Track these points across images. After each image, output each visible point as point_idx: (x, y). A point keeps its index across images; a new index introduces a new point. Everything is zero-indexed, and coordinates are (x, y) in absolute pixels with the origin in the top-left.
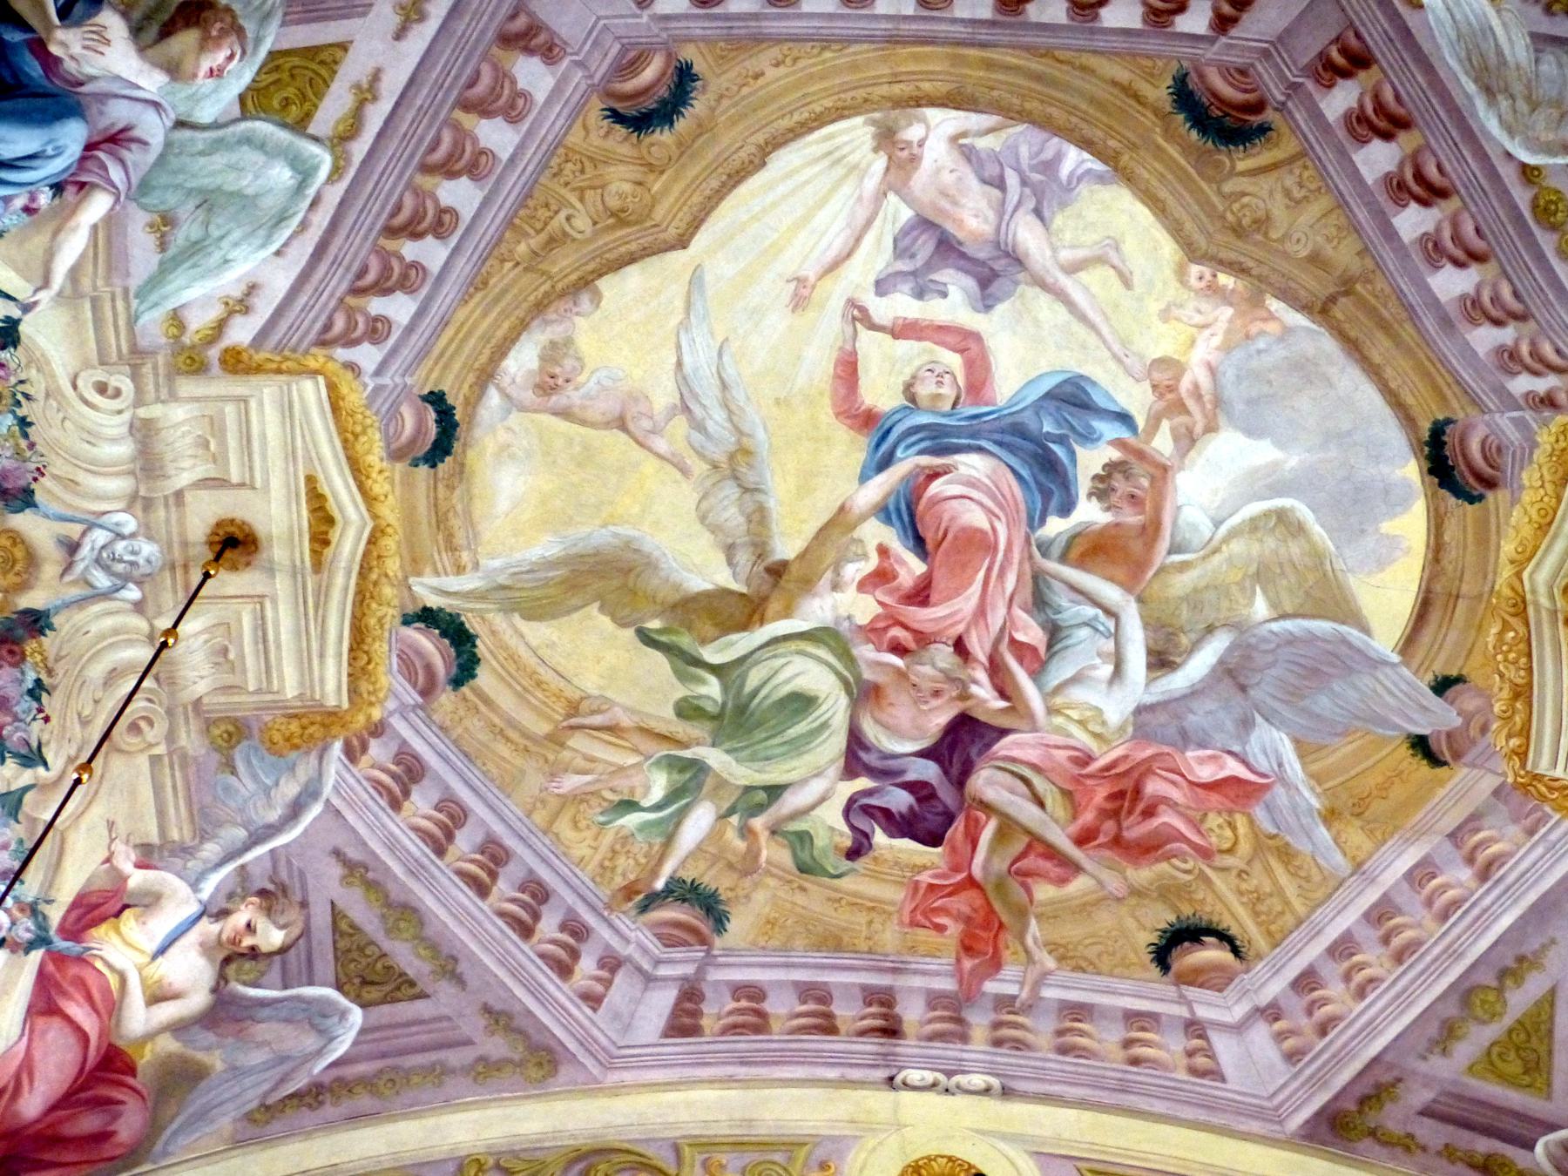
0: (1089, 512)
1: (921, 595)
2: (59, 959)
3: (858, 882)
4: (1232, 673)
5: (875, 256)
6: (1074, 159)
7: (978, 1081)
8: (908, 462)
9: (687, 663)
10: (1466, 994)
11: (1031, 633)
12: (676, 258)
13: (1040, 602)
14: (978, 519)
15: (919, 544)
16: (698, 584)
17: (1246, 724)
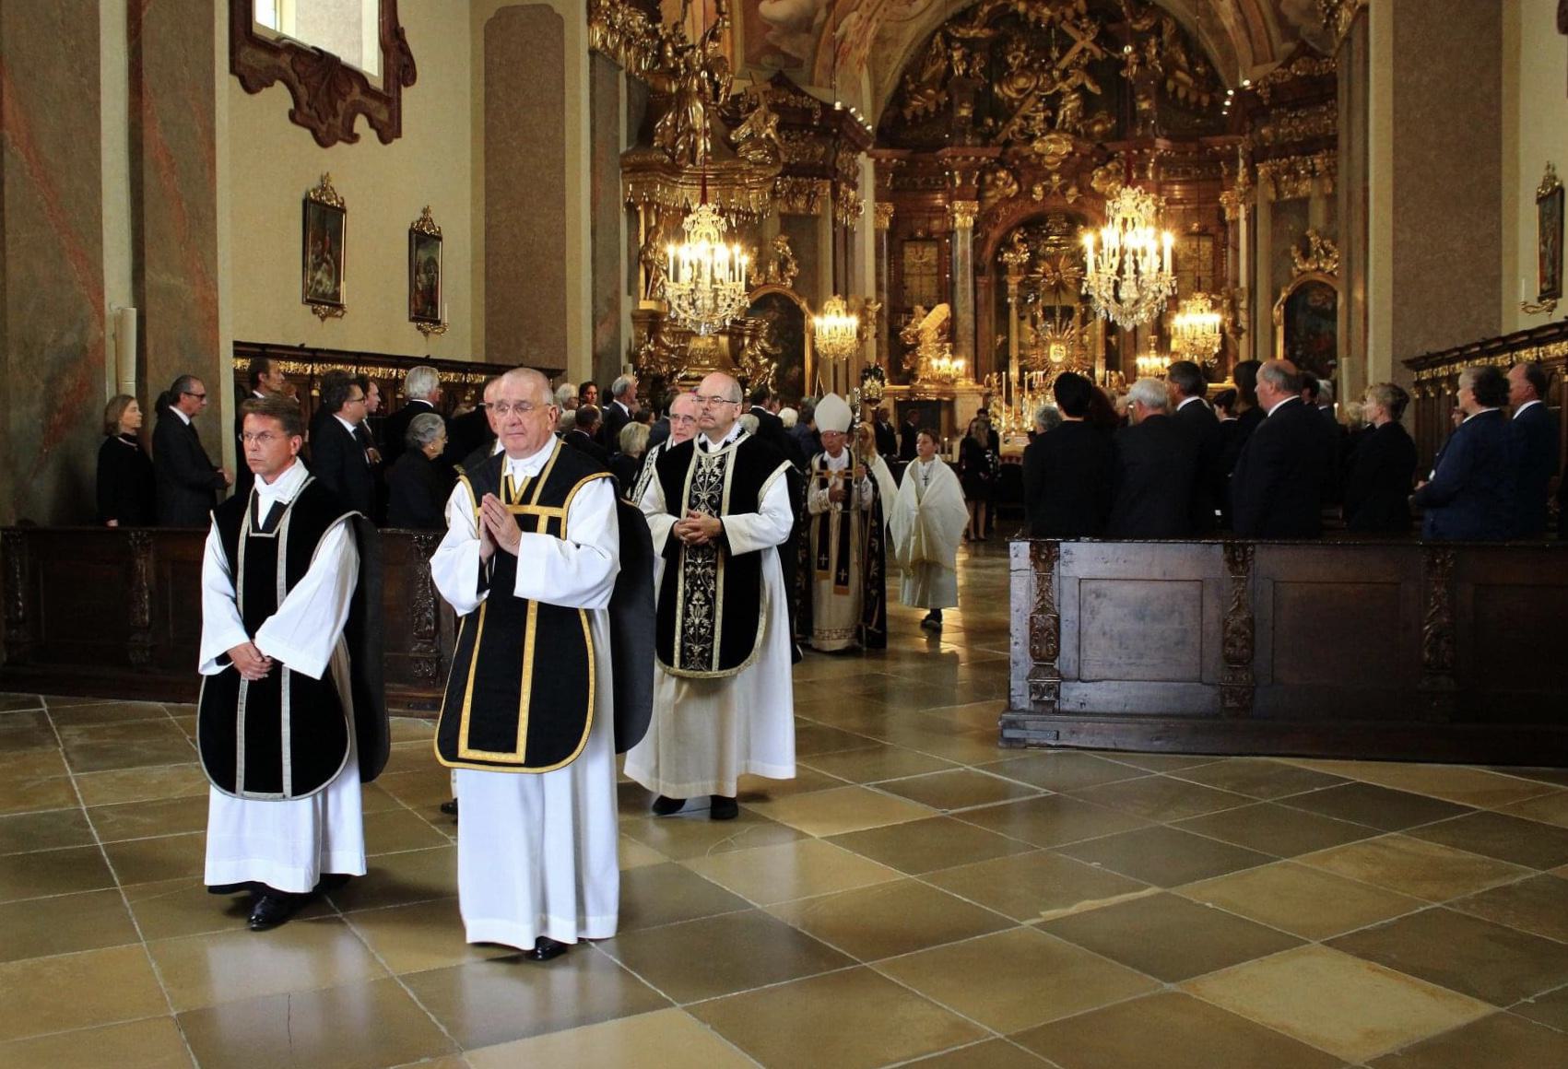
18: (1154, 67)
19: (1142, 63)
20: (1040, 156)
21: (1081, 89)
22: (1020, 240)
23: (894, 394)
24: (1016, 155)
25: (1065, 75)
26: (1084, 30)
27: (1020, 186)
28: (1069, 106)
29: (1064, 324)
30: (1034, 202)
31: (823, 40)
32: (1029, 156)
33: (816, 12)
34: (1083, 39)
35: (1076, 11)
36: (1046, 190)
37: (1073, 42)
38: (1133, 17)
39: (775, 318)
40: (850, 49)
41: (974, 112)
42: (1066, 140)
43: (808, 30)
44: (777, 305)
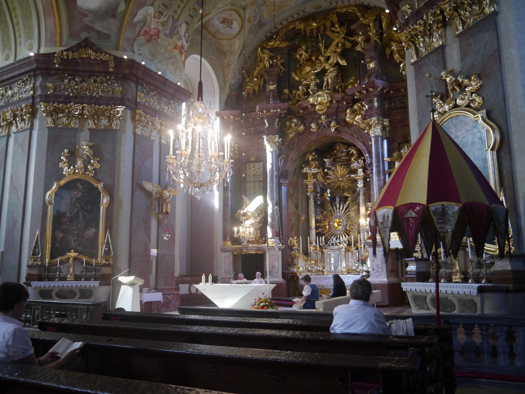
18: (374, 40)
19: (367, 40)
20: (313, 105)
21: (337, 64)
22: (313, 159)
23: (233, 251)
24: (300, 106)
25: (328, 59)
26: (338, 33)
27: (305, 125)
28: (331, 75)
29: (341, 207)
30: (313, 133)
31: (125, 22)
32: (307, 106)
34: (338, 37)
35: (332, 22)
36: (319, 126)
37: (332, 41)
38: (363, 16)
39: (79, 196)
40: (158, 35)
41: (277, 87)
42: (327, 93)
43: (114, 16)
44: (80, 187)
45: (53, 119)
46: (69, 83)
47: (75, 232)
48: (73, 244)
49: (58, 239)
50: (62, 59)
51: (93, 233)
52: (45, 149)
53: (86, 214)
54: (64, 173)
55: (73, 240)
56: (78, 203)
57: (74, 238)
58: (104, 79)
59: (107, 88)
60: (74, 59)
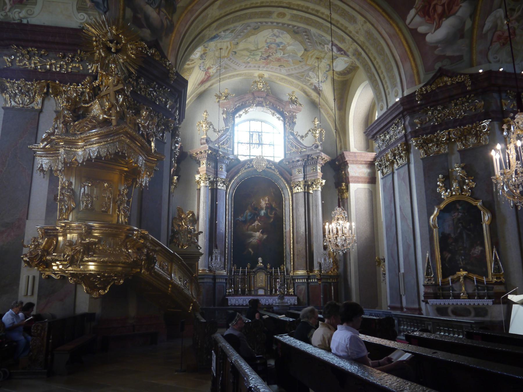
0: (281, 48)
1: (268, 50)
2: (207, 72)
3: (260, 61)
4: (289, 56)
5: (270, 35)
6: (285, 32)
7: (265, 70)
8: (269, 44)
9: (250, 53)
10: (299, 73)
11: (275, 52)
12: (256, 36)
13: (276, 51)
14: (273, 47)
15: (269, 48)
16: (253, 49)
17: (288, 58)
31: (475, 37)
33: (463, 24)
39: (459, 216)
43: (462, 36)
44: (460, 208)
45: (424, 150)
46: (432, 114)
47: (462, 252)
48: (462, 263)
49: (447, 259)
50: (422, 95)
51: (480, 251)
52: (422, 178)
53: (469, 233)
54: (443, 197)
55: (461, 259)
56: (460, 223)
57: (462, 257)
58: (464, 100)
59: (468, 107)
60: (432, 91)
